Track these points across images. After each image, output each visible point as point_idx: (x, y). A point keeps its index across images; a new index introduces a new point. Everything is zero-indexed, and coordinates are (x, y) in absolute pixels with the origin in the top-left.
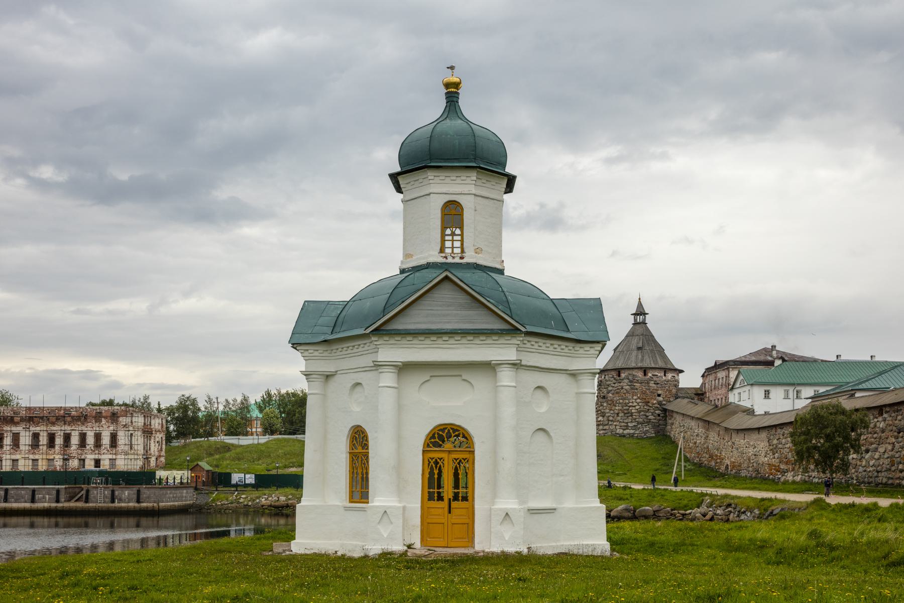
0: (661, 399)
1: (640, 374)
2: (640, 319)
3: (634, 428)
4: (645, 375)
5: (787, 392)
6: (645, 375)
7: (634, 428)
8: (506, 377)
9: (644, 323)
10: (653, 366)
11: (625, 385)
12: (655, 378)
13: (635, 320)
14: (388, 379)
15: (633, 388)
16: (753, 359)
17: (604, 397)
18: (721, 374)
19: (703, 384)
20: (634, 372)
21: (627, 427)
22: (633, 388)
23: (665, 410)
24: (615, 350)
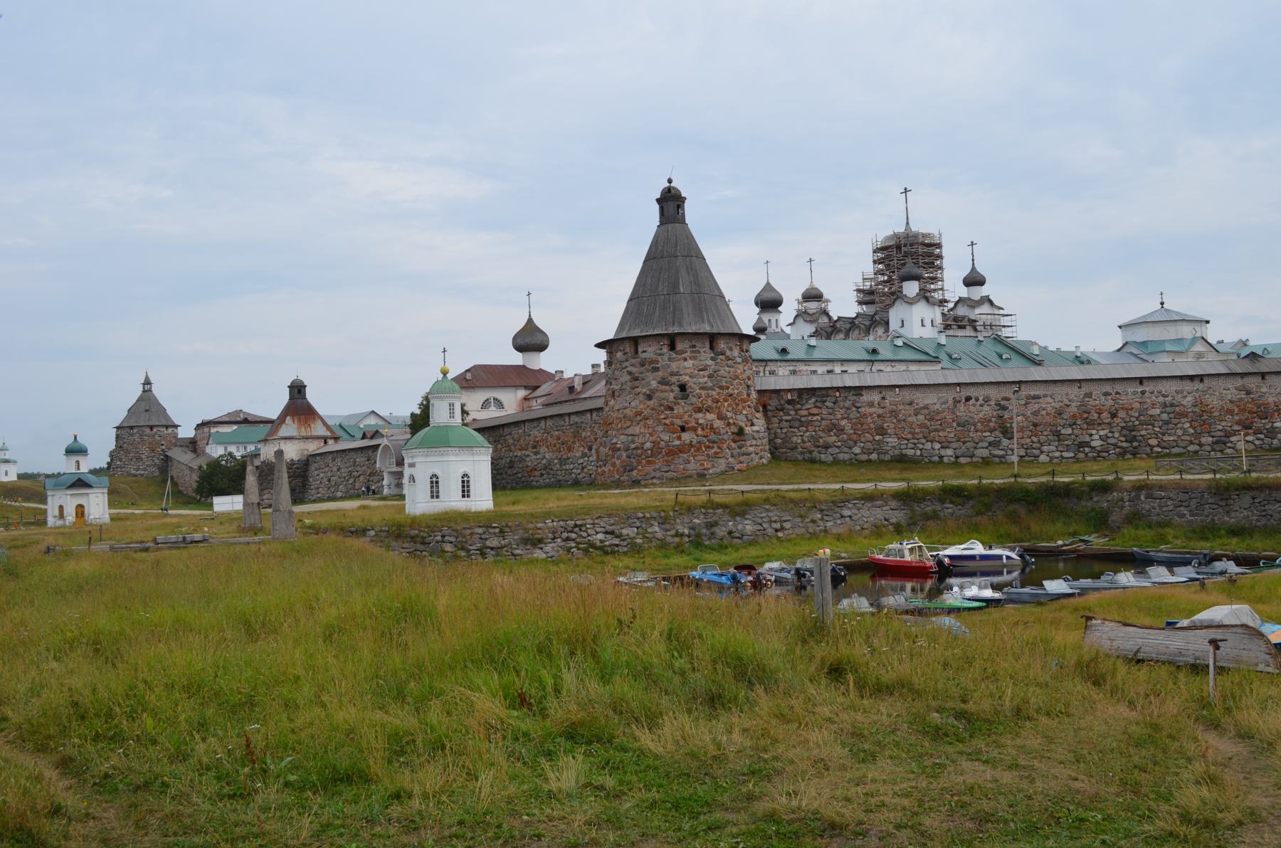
0: (163, 447)
1: (148, 430)
2: (147, 387)
3: (144, 469)
4: (152, 430)
5: (238, 447)
6: (152, 430)
7: (144, 469)
8: (91, 496)
9: (150, 390)
10: (157, 424)
11: (137, 437)
12: (159, 433)
13: (144, 388)
14: (69, 497)
15: (143, 440)
16: (227, 419)
17: (121, 447)
18: (206, 430)
19: (196, 435)
20: (143, 429)
21: (138, 469)
22: (143, 440)
23: (167, 456)
24: (129, 411)
